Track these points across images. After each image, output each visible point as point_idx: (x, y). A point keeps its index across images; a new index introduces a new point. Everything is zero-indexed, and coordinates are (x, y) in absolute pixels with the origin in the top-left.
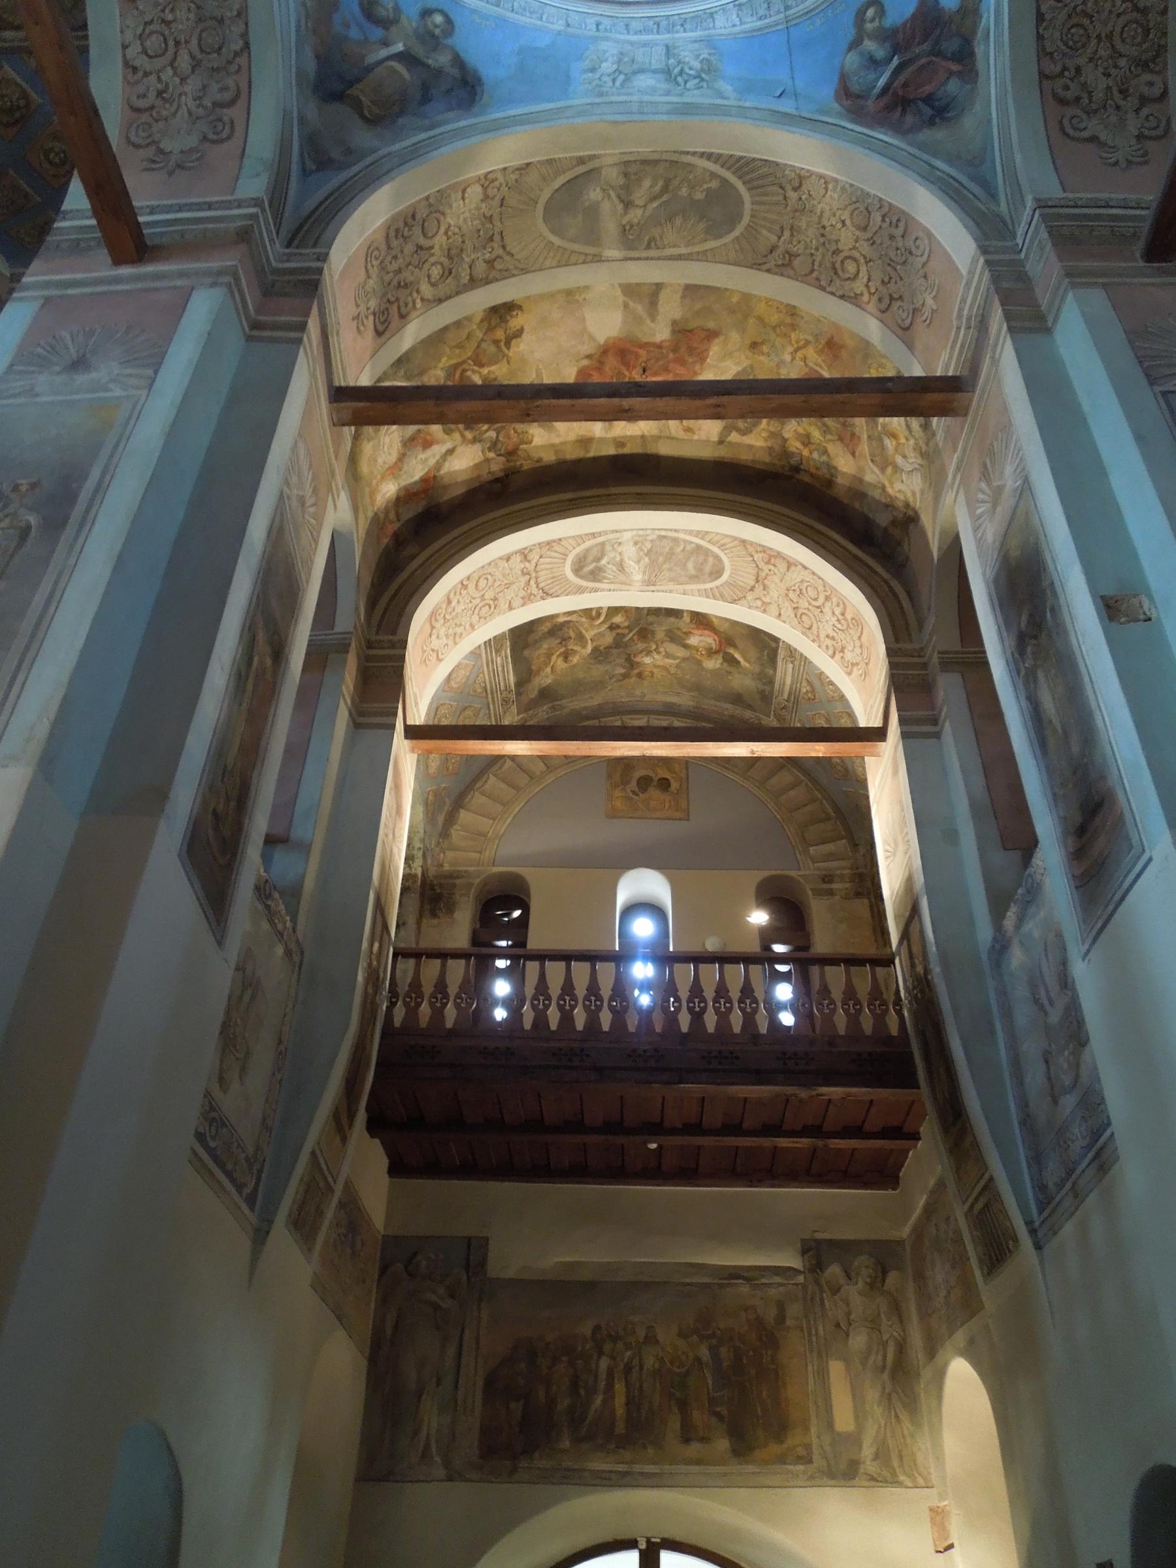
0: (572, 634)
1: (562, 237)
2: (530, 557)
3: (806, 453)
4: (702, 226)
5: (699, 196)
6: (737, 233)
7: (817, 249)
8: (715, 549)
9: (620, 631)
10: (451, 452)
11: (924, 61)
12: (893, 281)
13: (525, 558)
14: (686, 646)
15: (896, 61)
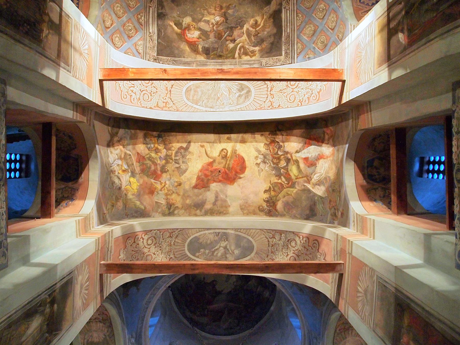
0: (253, 38)
1: (248, 239)
3: (156, 145)
4: (201, 241)
5: (202, 250)
7: (162, 242)
8: (190, 103)
9: (231, 38)
10: (297, 152)
14: (200, 29)
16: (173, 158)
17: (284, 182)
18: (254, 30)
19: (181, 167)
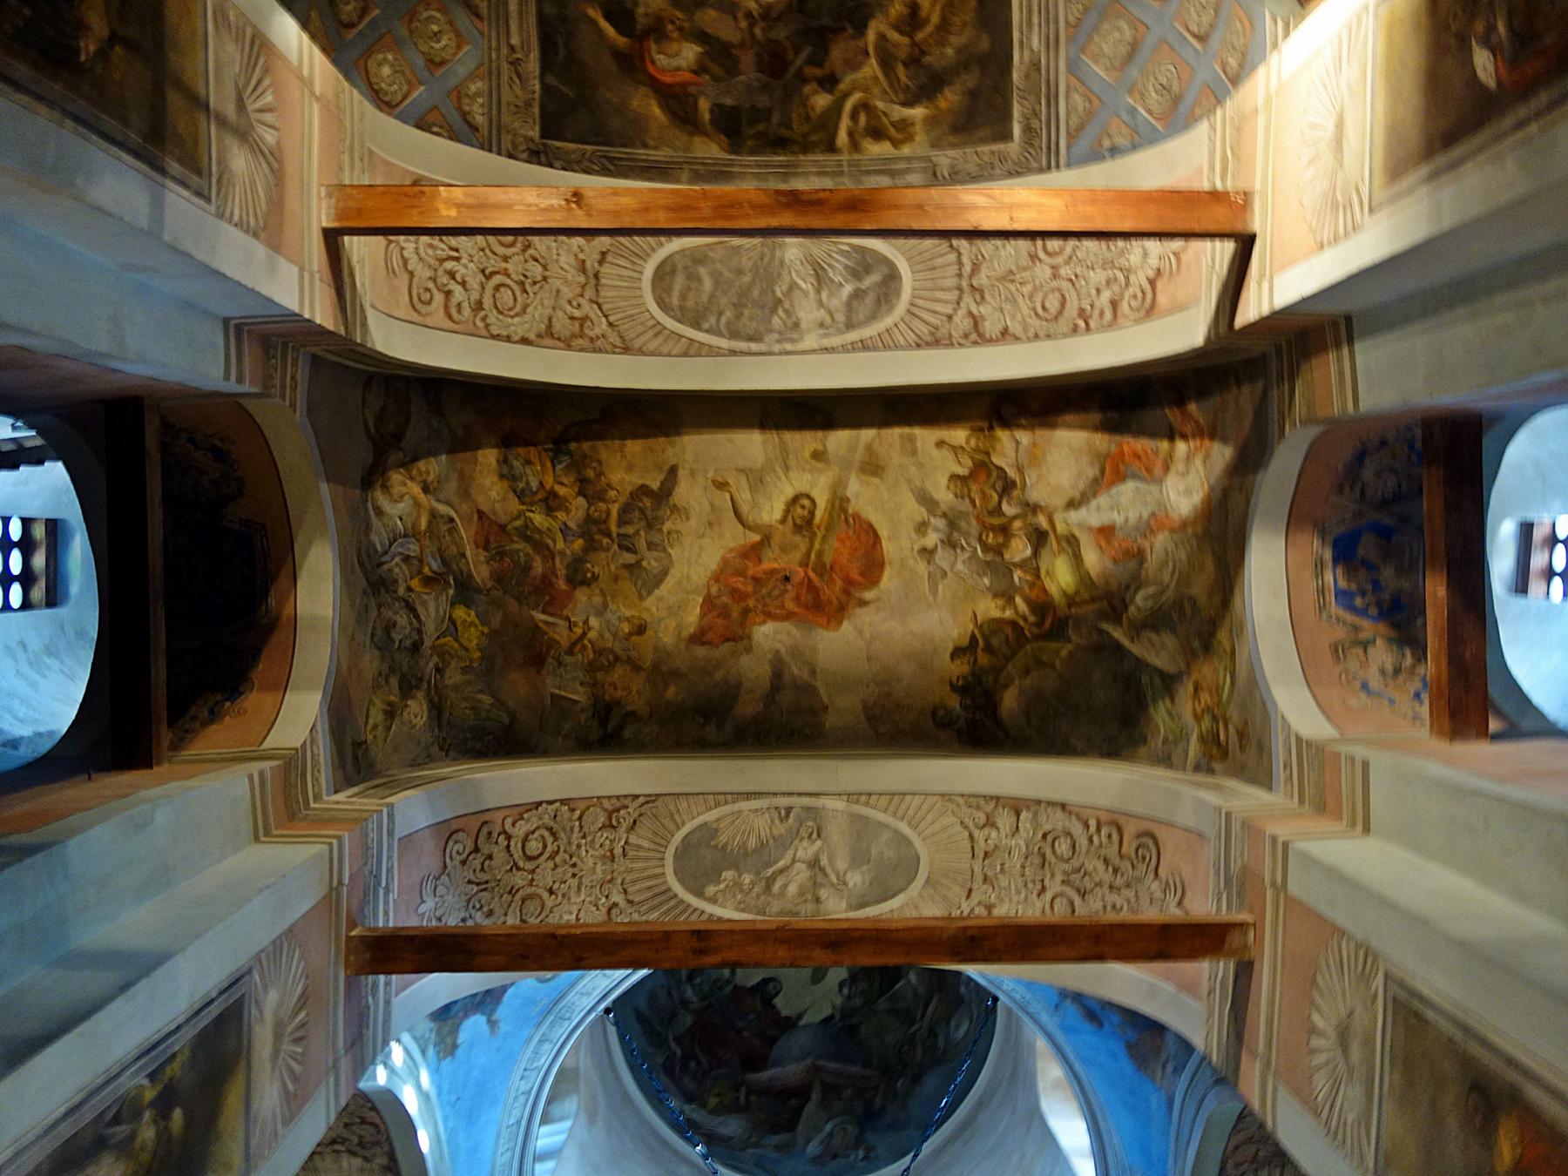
0: (901, 71)
1: (896, 831)
2: (967, 324)
4: (723, 839)
5: (728, 875)
7: (579, 846)
9: (818, 72)
10: (1072, 504)
13: (976, 321)
16: (614, 528)
17: (1025, 619)
18: (905, 40)
19: (644, 563)
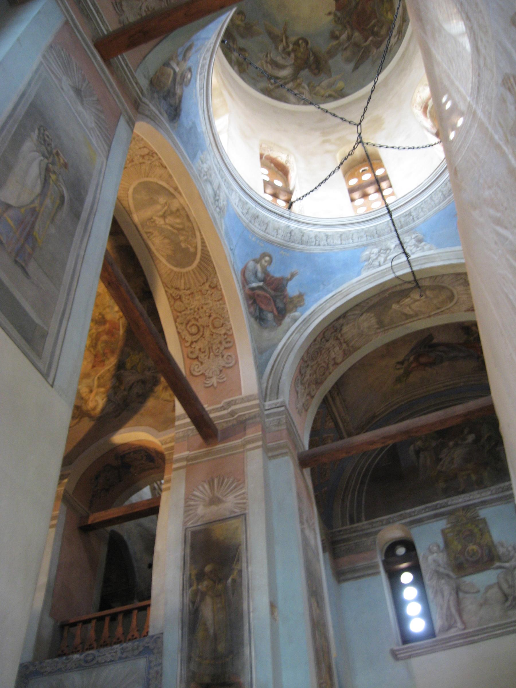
4: (170, 252)
5: (183, 245)
6: (175, 269)
7: (191, 309)
11: (268, 296)
12: (204, 354)
15: (261, 284)
